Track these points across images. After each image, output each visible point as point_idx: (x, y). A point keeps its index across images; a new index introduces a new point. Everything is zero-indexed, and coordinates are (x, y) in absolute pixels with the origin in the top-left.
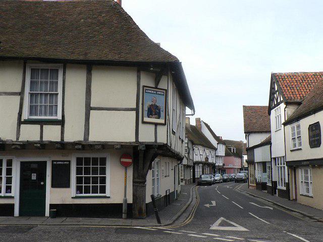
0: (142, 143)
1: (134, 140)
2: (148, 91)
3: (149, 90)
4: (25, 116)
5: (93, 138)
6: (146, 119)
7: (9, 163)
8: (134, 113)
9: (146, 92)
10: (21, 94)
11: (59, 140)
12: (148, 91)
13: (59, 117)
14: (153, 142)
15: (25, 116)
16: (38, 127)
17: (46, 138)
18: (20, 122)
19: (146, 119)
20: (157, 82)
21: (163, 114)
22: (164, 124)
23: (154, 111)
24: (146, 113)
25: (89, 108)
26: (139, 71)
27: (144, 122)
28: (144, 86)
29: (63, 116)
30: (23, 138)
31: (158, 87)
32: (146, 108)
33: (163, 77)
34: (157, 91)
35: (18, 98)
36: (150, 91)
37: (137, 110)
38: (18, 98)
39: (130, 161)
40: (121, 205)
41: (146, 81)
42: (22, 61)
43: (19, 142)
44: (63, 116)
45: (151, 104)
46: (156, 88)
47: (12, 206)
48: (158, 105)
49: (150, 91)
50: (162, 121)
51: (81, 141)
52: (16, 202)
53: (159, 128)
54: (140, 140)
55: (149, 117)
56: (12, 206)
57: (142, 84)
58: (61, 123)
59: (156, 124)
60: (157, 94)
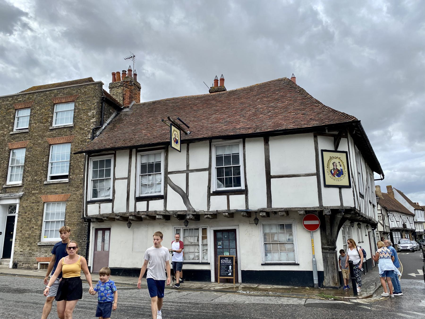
1: (318, 205)
5: (275, 205)
8: (315, 177)
10: (209, 169)
11: (244, 208)
15: (214, 188)
16: (224, 197)
17: (233, 207)
18: (210, 195)
20: (336, 145)
22: (349, 187)
25: (269, 177)
26: (315, 137)
27: (326, 186)
28: (322, 151)
29: (246, 186)
30: (213, 209)
31: (339, 149)
33: (342, 138)
37: (317, 174)
40: (311, 273)
42: (208, 141)
43: (211, 212)
44: (246, 186)
46: (336, 151)
47: (209, 272)
51: (264, 209)
52: (211, 268)
53: (343, 190)
54: (325, 204)
56: (209, 272)
57: (320, 148)
58: (245, 192)
59: (340, 187)
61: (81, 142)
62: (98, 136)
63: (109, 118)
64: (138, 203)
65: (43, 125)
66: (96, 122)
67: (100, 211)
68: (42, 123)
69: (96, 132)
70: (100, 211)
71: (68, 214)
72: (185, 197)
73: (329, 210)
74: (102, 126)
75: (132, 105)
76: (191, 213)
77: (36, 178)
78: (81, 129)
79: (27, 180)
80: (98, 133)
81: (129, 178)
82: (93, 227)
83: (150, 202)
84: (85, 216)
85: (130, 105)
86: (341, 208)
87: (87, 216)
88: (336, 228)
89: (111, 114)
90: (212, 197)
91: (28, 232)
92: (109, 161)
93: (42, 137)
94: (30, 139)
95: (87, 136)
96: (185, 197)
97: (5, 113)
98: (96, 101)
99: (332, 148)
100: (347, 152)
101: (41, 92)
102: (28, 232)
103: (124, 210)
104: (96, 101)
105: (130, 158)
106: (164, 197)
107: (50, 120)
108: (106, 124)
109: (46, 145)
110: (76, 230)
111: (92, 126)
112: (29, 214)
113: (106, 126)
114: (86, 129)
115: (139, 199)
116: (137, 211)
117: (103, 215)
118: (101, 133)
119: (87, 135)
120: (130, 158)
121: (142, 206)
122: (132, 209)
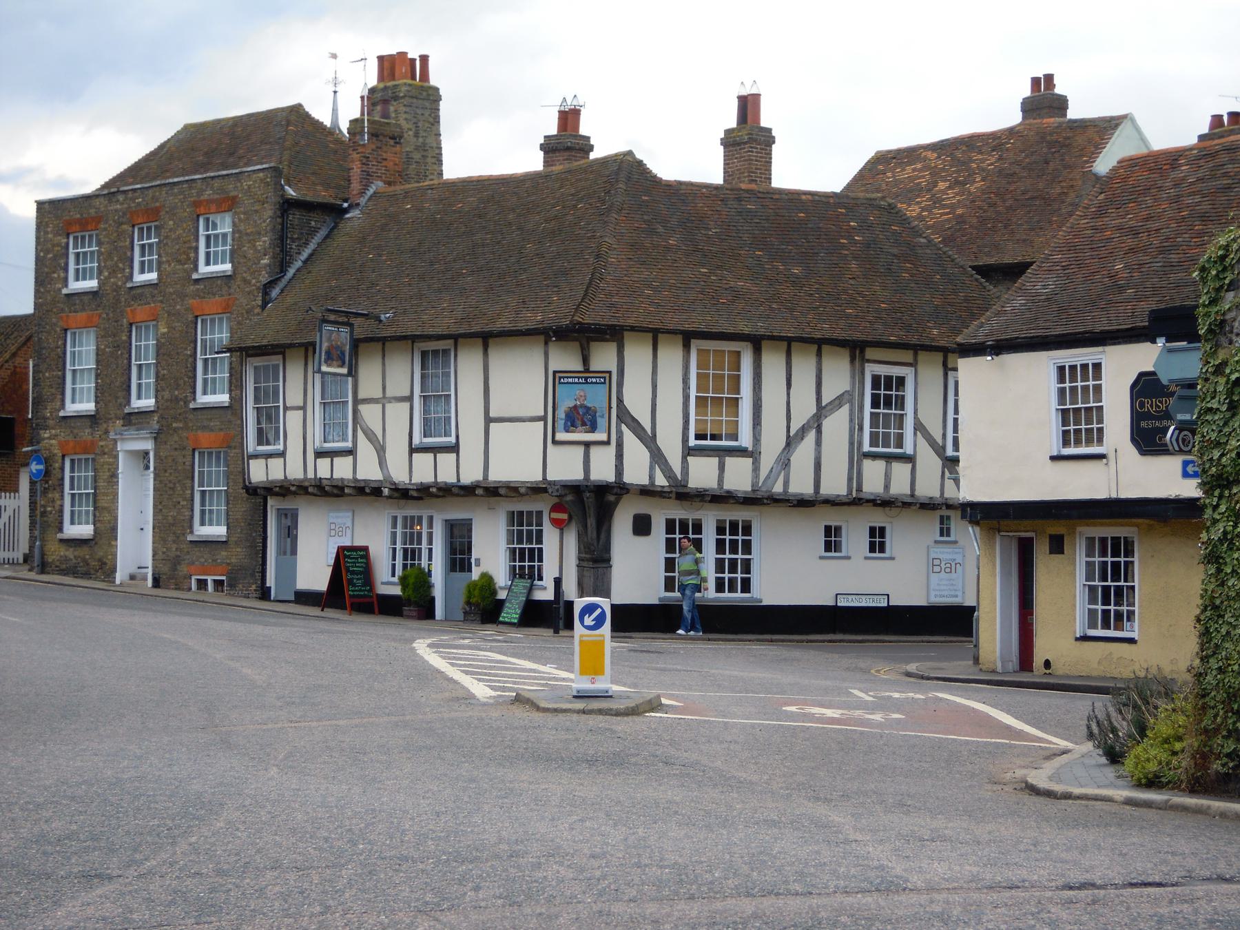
0: (550, 483)
2: (566, 380)
3: (568, 377)
4: (416, 441)
6: (561, 436)
7: (431, 519)
9: (560, 383)
10: (410, 399)
12: (566, 380)
13: (453, 439)
14: (580, 481)
15: (416, 441)
16: (431, 455)
18: (413, 450)
19: (561, 436)
20: (586, 361)
21: (602, 423)
22: (608, 443)
23: (581, 418)
24: (560, 424)
25: (489, 420)
27: (554, 442)
28: (555, 372)
29: (457, 437)
32: (561, 414)
34: (586, 378)
35: (407, 405)
36: (570, 380)
38: (407, 405)
39: (564, 516)
41: (565, 359)
43: (413, 484)
44: (457, 437)
45: (572, 405)
48: (589, 405)
49: (570, 380)
50: (604, 437)
55: (567, 431)
58: (454, 448)
59: (587, 445)
60: (587, 383)
61: (247, 312)
62: (276, 299)
63: (306, 244)
64: (319, 460)
65: (181, 267)
66: (269, 265)
67: (267, 475)
68: (179, 262)
69: (270, 291)
70: (267, 475)
71: (232, 477)
72: (381, 450)
73: (556, 487)
74: (285, 274)
75: (367, 197)
76: (388, 485)
77: (176, 393)
78: (245, 281)
79: (163, 398)
80: (275, 293)
81: (303, 408)
82: (272, 506)
83: (335, 459)
84: (247, 484)
85: (362, 199)
86: (585, 483)
87: (250, 483)
88: (591, 522)
89: (314, 231)
90: (414, 455)
91: (172, 513)
92: (276, 367)
93: (183, 296)
94: (161, 302)
95: (255, 300)
96: (381, 450)
97: (115, 235)
98: (268, 212)
99: (581, 369)
100: (610, 373)
101: (174, 184)
102: (172, 513)
103: (300, 476)
104: (270, 213)
105: (306, 364)
106: (351, 452)
107: (192, 255)
108: (299, 264)
109: (190, 317)
110: (245, 511)
111: (264, 278)
112: (171, 474)
113: (298, 270)
114: (254, 281)
115: (319, 454)
116: (318, 477)
117: (272, 482)
118: (282, 291)
119: (257, 296)
120: (306, 364)
121: (323, 469)
122: (311, 475)
